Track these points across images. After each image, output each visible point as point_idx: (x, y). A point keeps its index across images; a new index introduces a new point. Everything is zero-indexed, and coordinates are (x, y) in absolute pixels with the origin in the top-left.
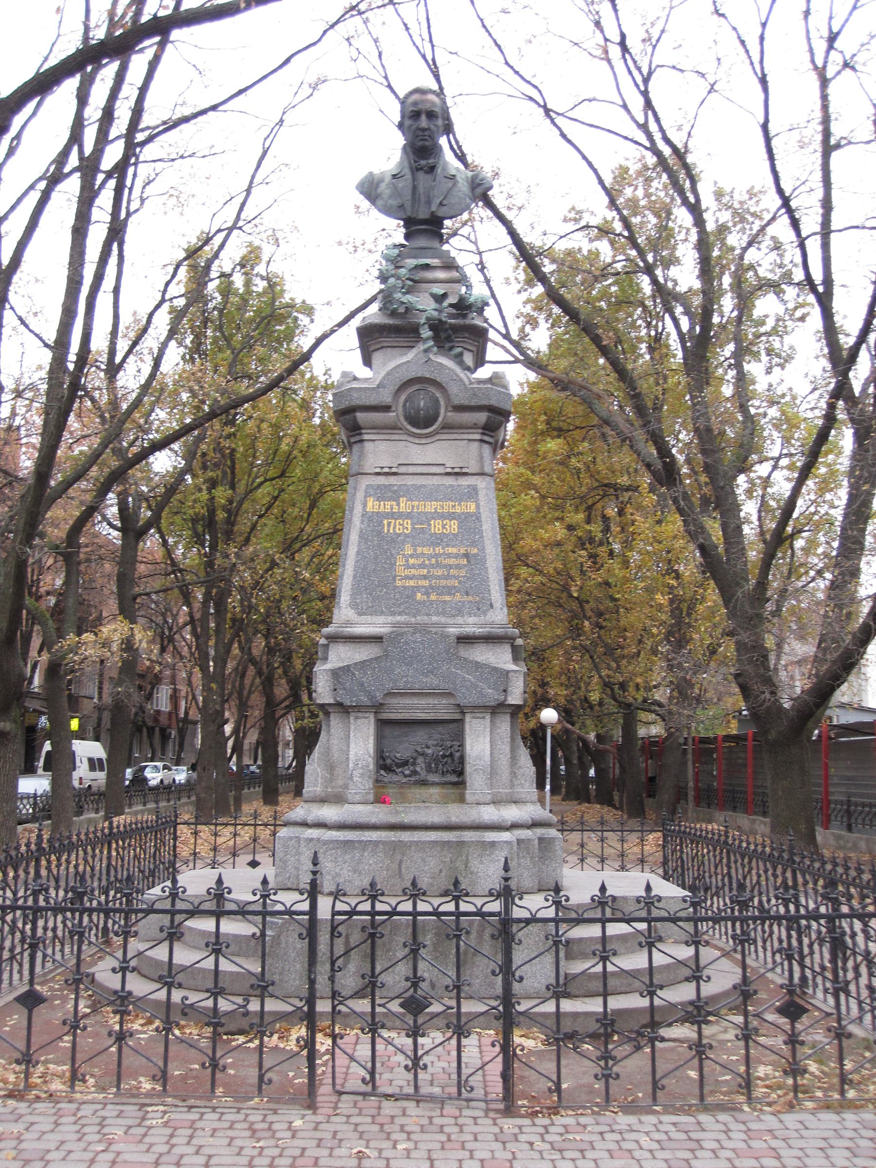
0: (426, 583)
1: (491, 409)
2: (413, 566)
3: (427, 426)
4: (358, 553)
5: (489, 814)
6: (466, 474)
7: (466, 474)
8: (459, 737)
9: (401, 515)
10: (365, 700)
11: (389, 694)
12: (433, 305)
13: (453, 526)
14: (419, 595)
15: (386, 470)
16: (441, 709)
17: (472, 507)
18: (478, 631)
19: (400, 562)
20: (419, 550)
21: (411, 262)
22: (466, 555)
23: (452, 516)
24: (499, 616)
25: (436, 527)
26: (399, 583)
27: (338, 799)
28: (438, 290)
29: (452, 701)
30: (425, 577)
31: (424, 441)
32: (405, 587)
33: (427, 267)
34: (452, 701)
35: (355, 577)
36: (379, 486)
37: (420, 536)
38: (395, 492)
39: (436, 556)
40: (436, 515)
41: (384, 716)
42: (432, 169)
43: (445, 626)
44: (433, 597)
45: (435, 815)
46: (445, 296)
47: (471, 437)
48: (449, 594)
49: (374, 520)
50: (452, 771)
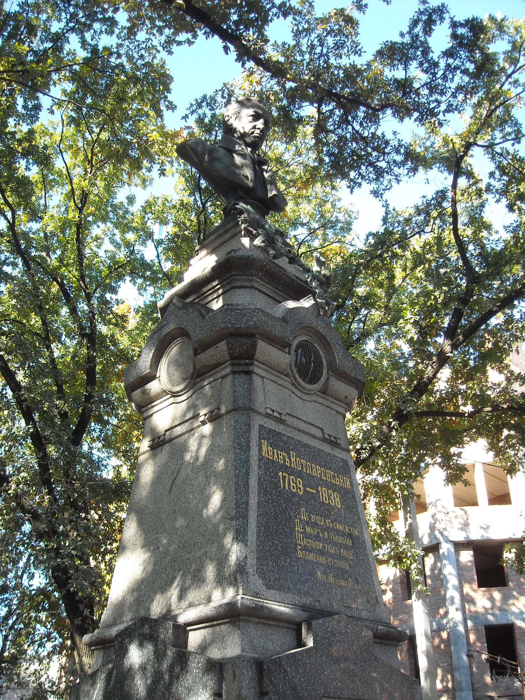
4: (259, 504)
36: (270, 430)
38: (285, 443)
39: (327, 529)
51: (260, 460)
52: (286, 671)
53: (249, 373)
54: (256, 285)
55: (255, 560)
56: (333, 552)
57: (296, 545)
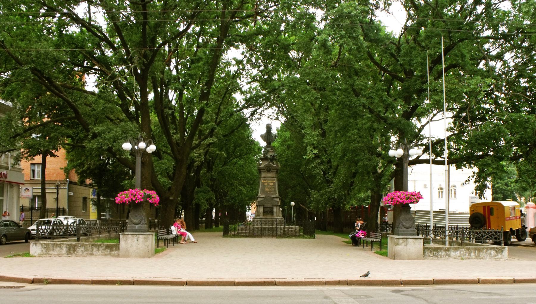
5: (276, 217)
24: (278, 195)
27: (259, 216)
37: (268, 185)
45: (270, 218)
49: (263, 183)
50: (272, 213)
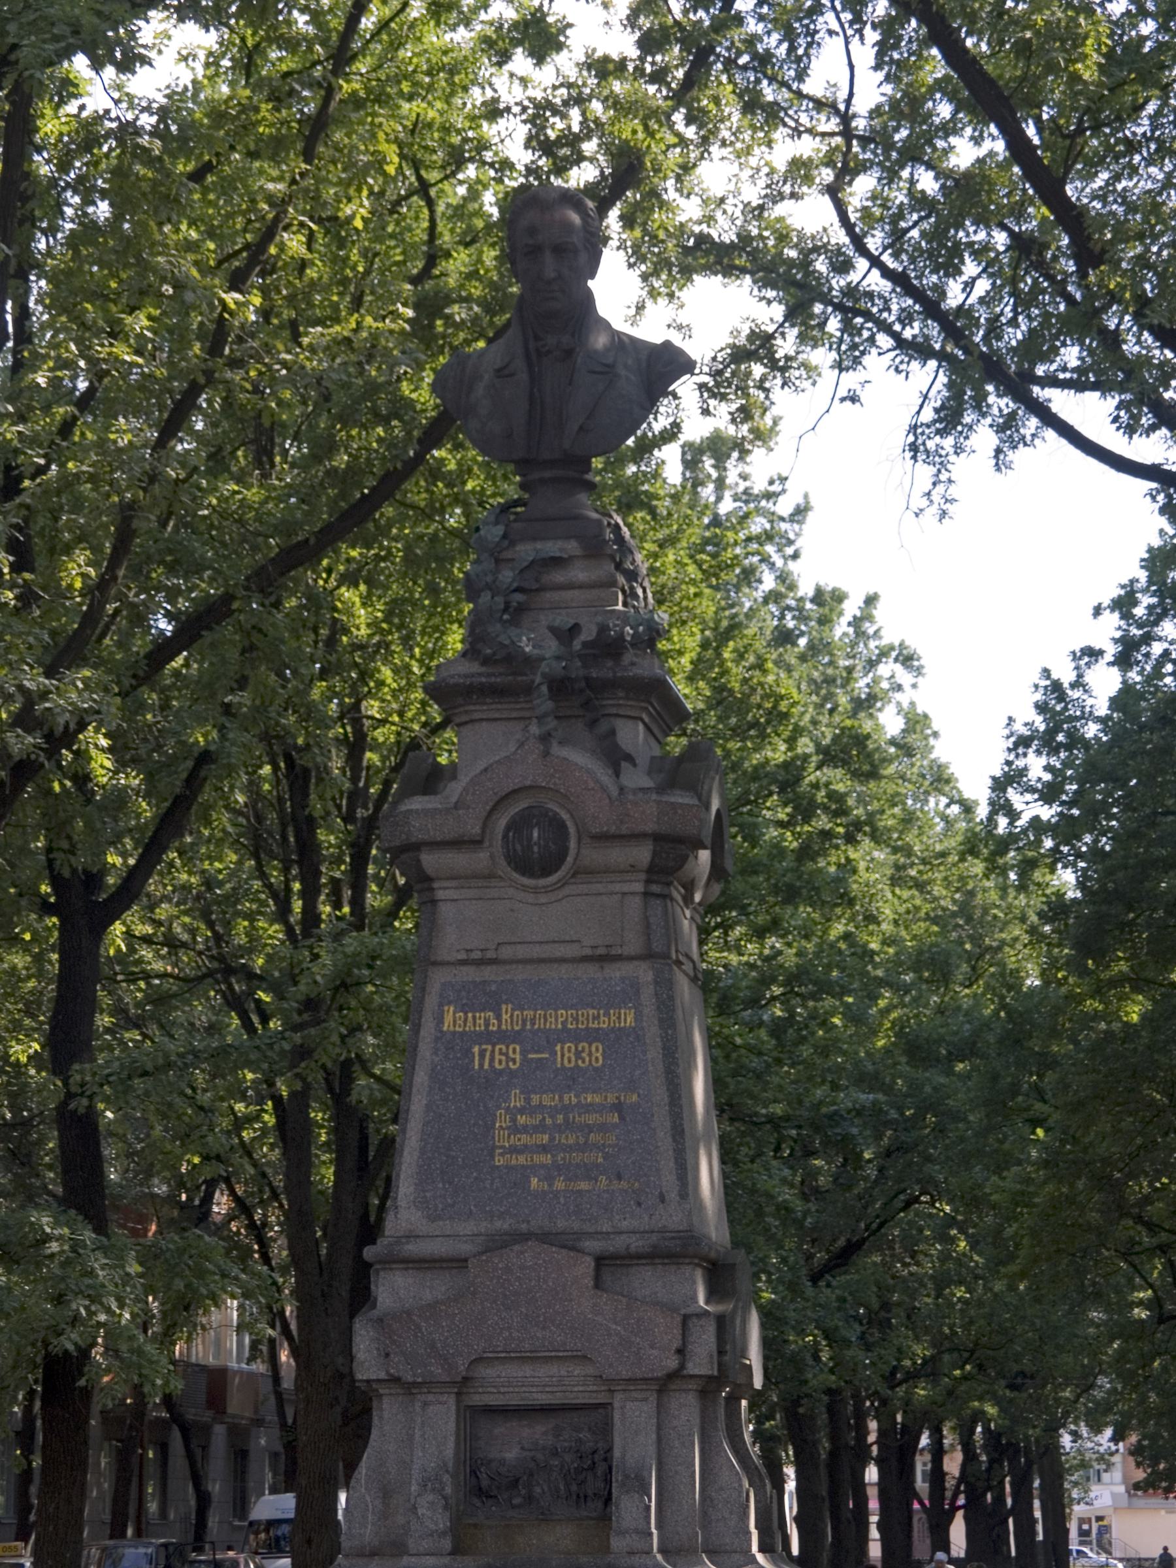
0: (547, 1159)
1: (658, 838)
2: (525, 1129)
3: (546, 872)
4: (428, 1108)
6: (619, 958)
7: (619, 958)
8: (605, 1430)
9: (503, 1037)
10: (437, 1371)
11: (480, 1360)
12: (552, 646)
13: (596, 1054)
14: (534, 1181)
15: (477, 955)
16: (570, 1383)
17: (629, 1019)
18: (637, 1244)
19: (502, 1121)
20: (535, 1099)
21: (526, 551)
22: (618, 1107)
23: (592, 1036)
25: (565, 1055)
26: (499, 1161)
28: (563, 620)
29: (591, 1370)
30: (544, 1149)
31: (543, 899)
32: (510, 1168)
33: (557, 562)
34: (591, 1370)
35: (423, 1151)
39: (567, 1109)
40: (565, 1035)
41: (477, 1400)
42: (569, 353)
43: (581, 1235)
44: (559, 1185)
46: (575, 629)
47: (626, 888)
48: (588, 1178)
49: (457, 1046)
51: (437, 1039)
52: (418, 1327)
53: (434, 902)
54: (476, 716)
55: (412, 1189)
56: (571, 1141)
57: (494, 1148)
